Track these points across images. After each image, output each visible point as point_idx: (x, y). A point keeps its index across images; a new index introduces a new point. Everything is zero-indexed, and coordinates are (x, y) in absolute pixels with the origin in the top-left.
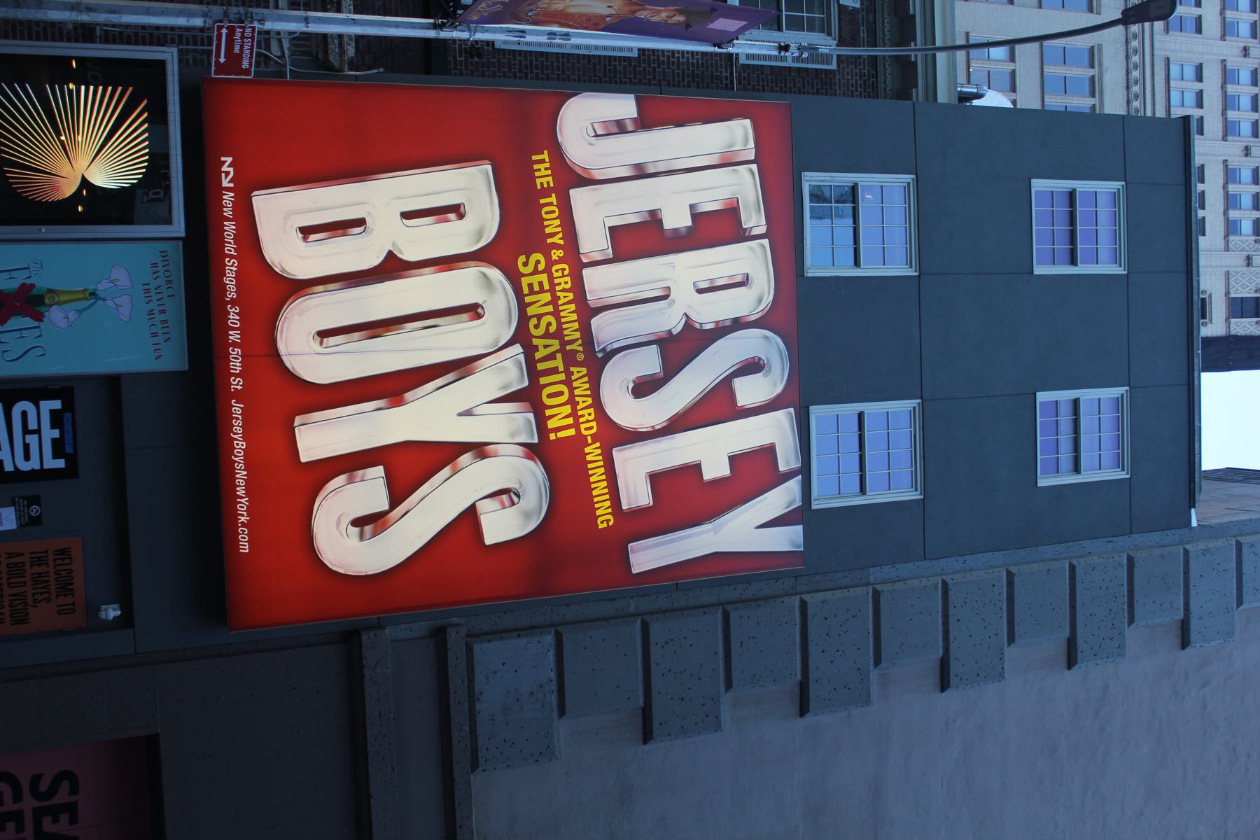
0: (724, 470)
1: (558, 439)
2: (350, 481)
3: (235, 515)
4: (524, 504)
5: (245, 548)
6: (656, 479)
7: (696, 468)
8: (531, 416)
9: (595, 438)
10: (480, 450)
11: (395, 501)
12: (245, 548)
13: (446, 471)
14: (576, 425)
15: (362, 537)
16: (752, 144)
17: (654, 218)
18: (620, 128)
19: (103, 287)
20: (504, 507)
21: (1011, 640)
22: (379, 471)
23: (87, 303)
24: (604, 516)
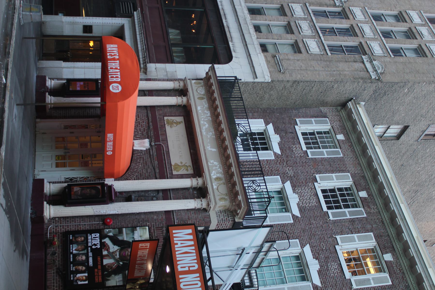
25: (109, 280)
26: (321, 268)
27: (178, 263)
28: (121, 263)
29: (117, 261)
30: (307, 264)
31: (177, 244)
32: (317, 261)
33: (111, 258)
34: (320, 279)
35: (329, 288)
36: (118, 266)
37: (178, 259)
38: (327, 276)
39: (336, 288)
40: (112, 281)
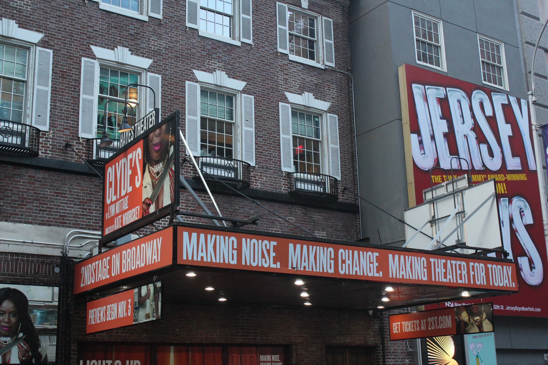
0: (509, 126)
1: (507, 190)
2: (522, 270)
3: (532, 312)
4: (523, 207)
5: (539, 310)
6: (514, 155)
7: (509, 137)
8: (502, 199)
9: (505, 176)
10: (511, 221)
11: (526, 256)
12: (539, 310)
13: (517, 234)
14: (502, 182)
15: (534, 268)
16: (419, 86)
17: (445, 135)
18: (421, 142)
19: (475, 354)
20: (524, 215)
21: (538, 19)
22: (519, 258)
23: (480, 360)
24: (523, 177)
25: (46, 356)
26: (16, 20)
27: (227, 262)
28: (21, 335)
29: (16, 341)
30: (5, 37)
31: (202, 258)
32: (3, 18)
33: (10, 351)
34: (32, 30)
35: (48, 25)
36: (26, 340)
37: (321, 271)
38: (30, 17)
39: (50, 14)
40: (48, 352)
